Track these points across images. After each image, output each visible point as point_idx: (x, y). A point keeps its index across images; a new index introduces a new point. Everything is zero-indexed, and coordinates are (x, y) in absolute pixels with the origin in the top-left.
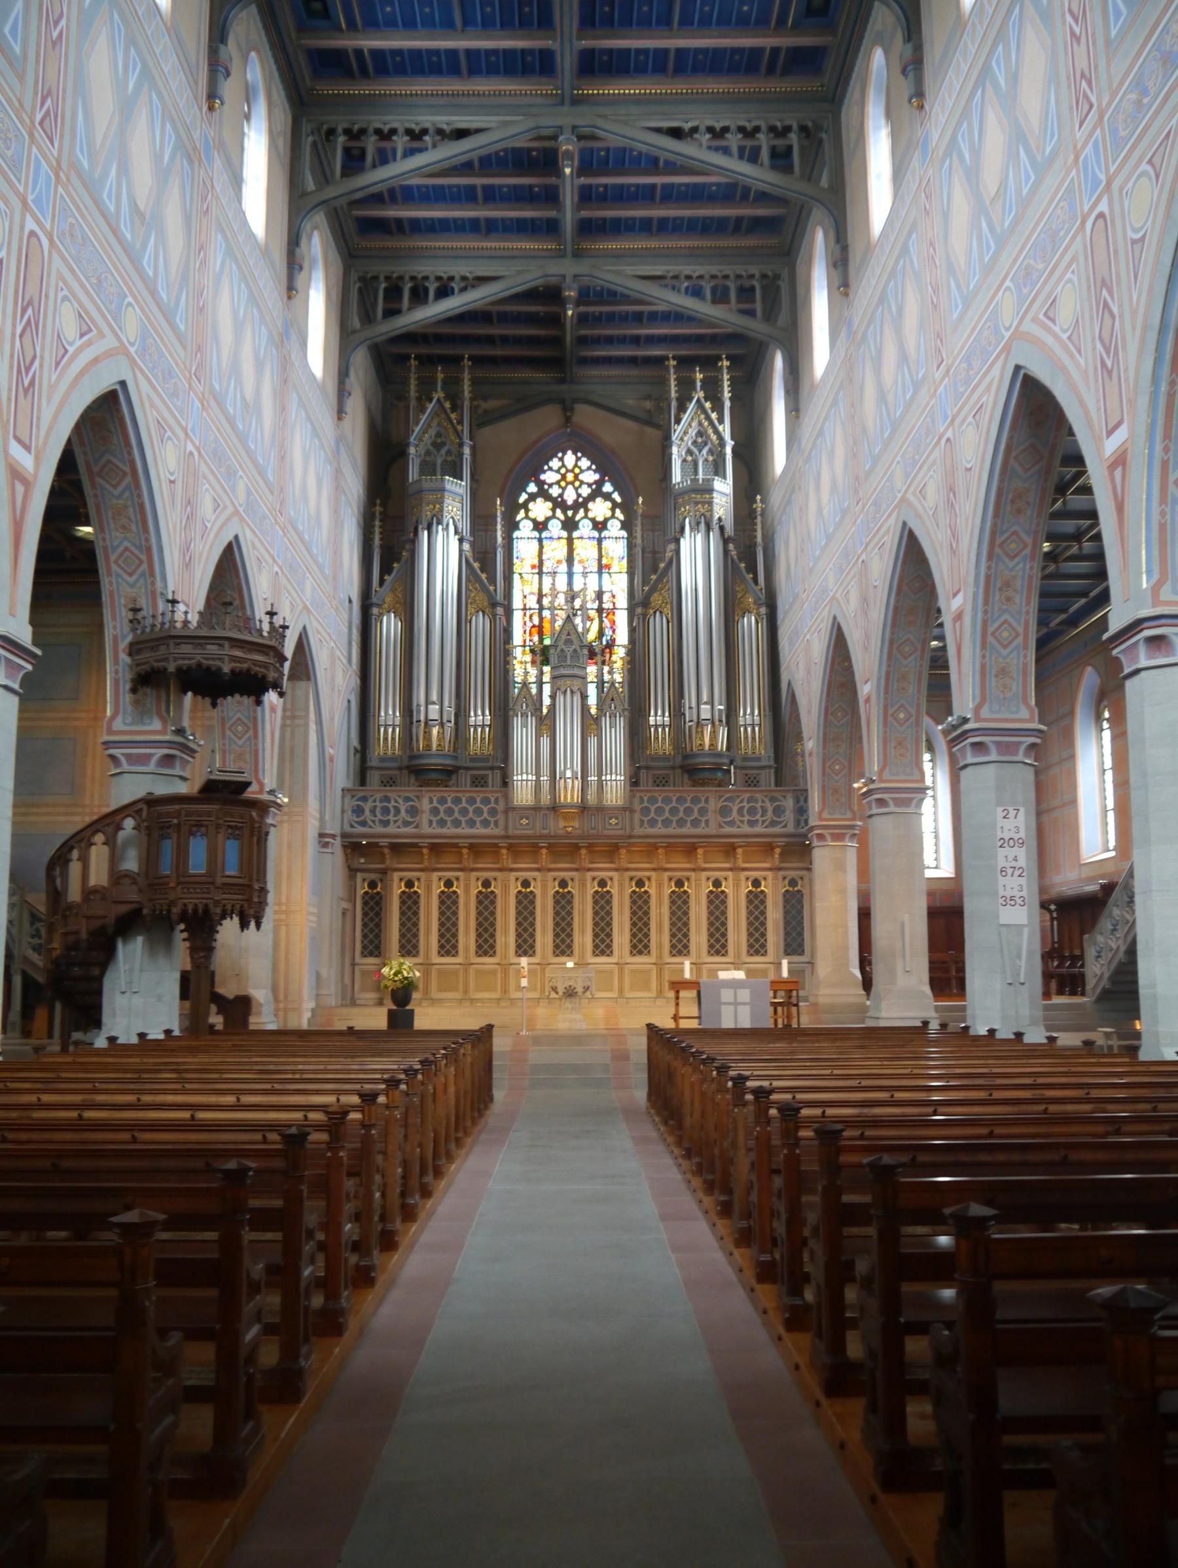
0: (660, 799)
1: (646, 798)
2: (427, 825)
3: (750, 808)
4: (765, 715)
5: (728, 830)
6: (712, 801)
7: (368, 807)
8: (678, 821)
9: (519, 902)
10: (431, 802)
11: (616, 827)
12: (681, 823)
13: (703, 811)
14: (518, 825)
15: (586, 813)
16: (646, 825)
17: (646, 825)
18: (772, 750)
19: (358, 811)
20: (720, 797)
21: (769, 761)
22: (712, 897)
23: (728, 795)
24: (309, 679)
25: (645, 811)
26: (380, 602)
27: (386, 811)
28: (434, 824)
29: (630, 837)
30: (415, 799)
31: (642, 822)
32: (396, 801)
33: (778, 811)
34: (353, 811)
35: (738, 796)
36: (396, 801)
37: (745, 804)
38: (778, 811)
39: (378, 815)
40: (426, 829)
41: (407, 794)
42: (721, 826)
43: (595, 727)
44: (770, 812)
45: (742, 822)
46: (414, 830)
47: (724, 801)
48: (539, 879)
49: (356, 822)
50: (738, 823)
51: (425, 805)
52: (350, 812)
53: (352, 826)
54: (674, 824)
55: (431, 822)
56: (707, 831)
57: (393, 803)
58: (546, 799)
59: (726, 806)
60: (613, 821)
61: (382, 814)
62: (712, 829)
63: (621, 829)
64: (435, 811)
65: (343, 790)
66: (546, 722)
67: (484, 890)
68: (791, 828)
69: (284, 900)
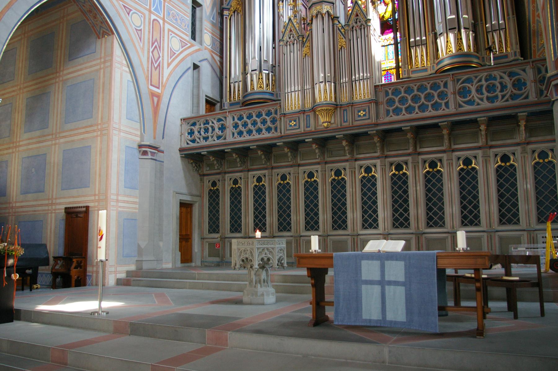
0: (402, 90)
1: (390, 92)
2: (231, 136)
3: (488, 86)
4: (509, 19)
5: (468, 108)
6: (450, 84)
7: (196, 129)
8: (419, 107)
9: (306, 189)
10: (234, 119)
11: (364, 118)
12: (423, 108)
13: (442, 95)
14: (288, 126)
15: (338, 109)
16: (391, 114)
17: (391, 114)
18: (518, 46)
19: (191, 133)
20: (458, 80)
21: (515, 55)
22: (463, 174)
23: (465, 77)
24: (113, 33)
25: (390, 102)
26: (228, 7)
27: (206, 130)
28: (236, 135)
29: (377, 125)
30: (224, 119)
31: (388, 112)
32: (213, 123)
33: (519, 84)
34: (189, 133)
35: (476, 77)
36: (213, 123)
37: (483, 82)
38: (519, 84)
39: (202, 133)
40: (230, 139)
41: (219, 117)
42: (460, 106)
43: (344, 40)
44: (509, 85)
45: (482, 100)
46: (223, 141)
47: (463, 83)
48: (319, 170)
49: (190, 141)
50: (477, 100)
51: (229, 122)
52: (187, 135)
53: (188, 144)
54: (417, 110)
55: (233, 134)
56: (447, 111)
57: (211, 124)
58: (309, 105)
59: (464, 88)
60: (362, 113)
61: (205, 133)
62: (452, 109)
63: (369, 119)
64: (236, 126)
65: (181, 120)
66: (306, 45)
67: (282, 182)
68: (533, 98)
69: (97, 193)
